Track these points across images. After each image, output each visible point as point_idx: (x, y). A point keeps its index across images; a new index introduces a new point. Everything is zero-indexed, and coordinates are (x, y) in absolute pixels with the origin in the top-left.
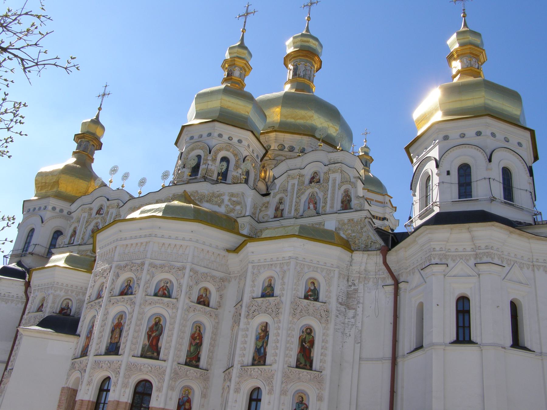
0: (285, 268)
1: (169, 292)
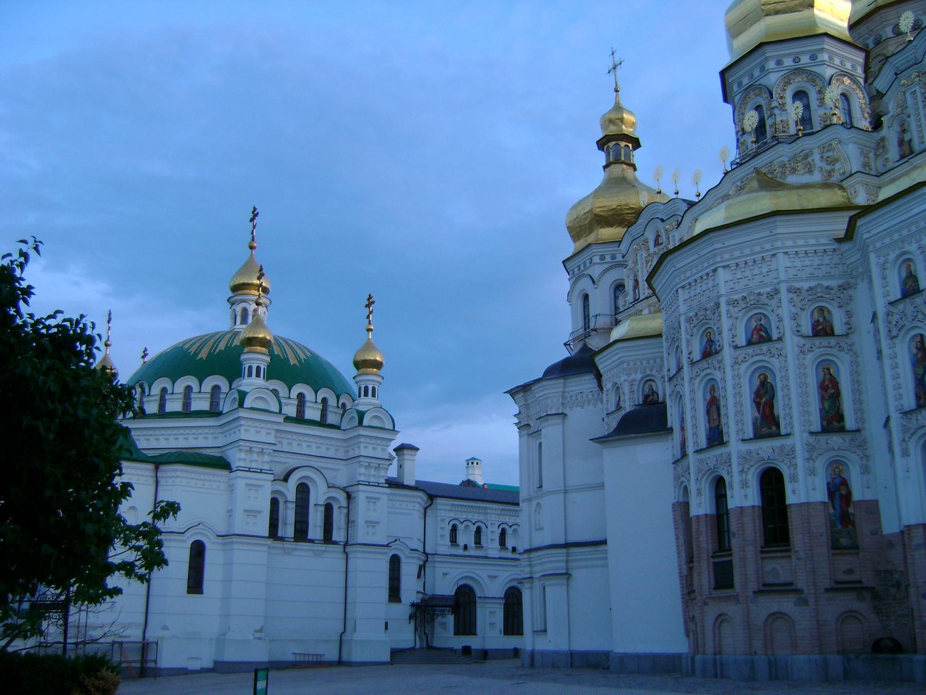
1: (766, 332)
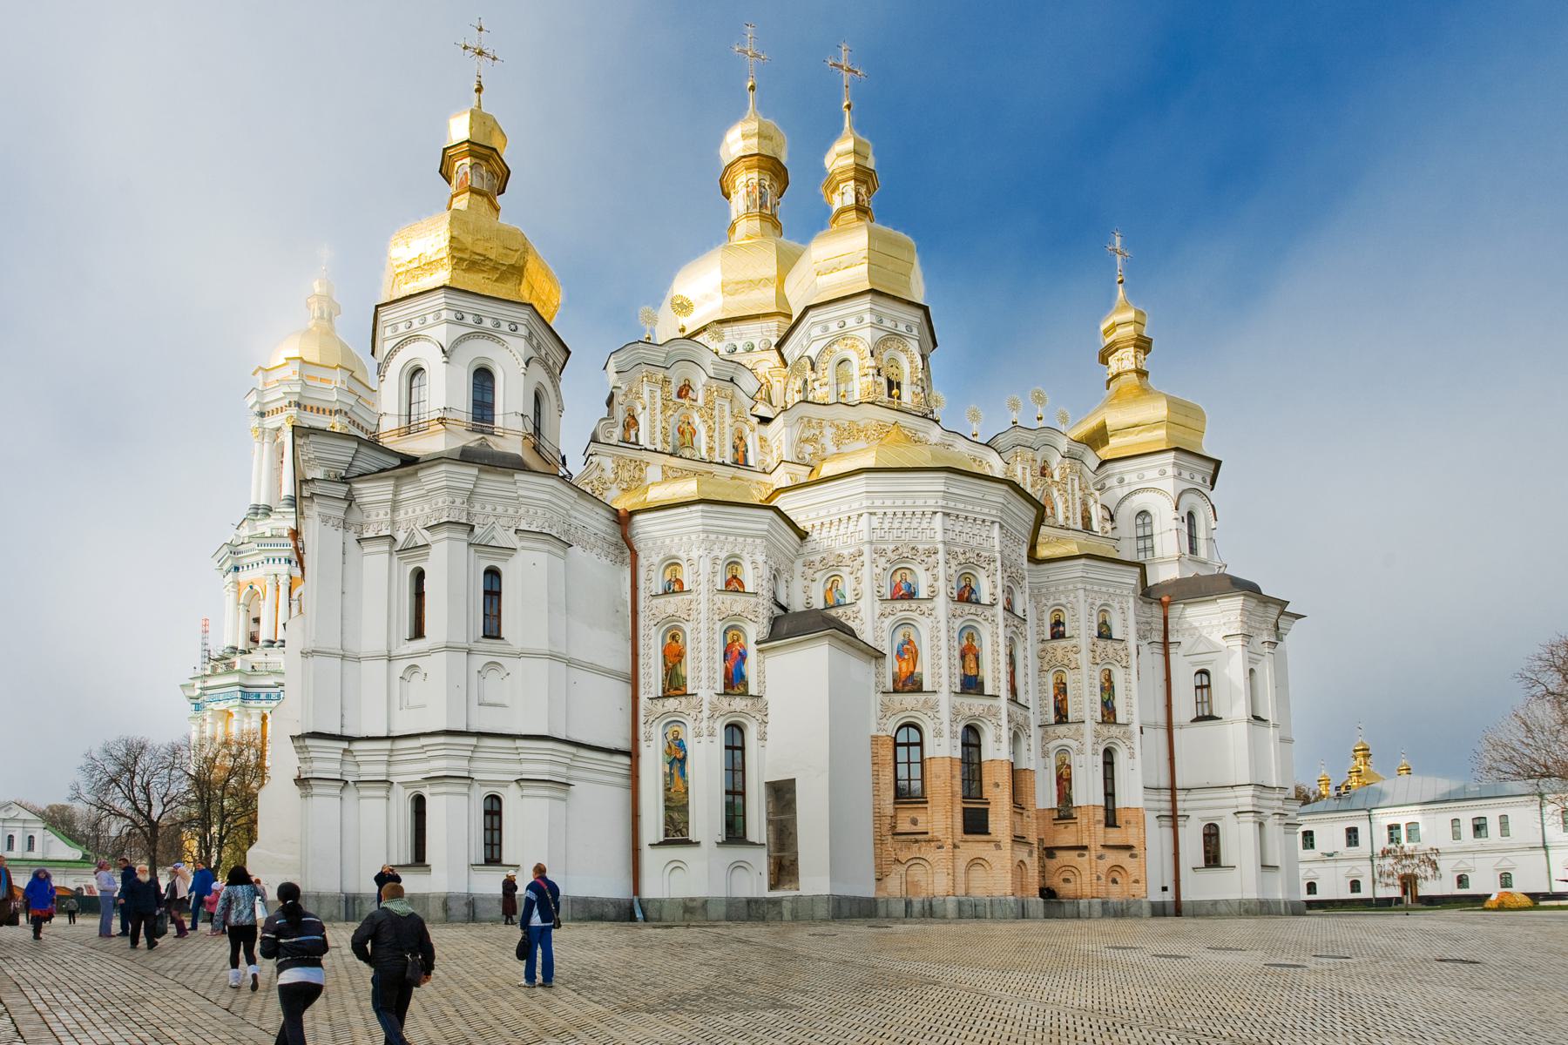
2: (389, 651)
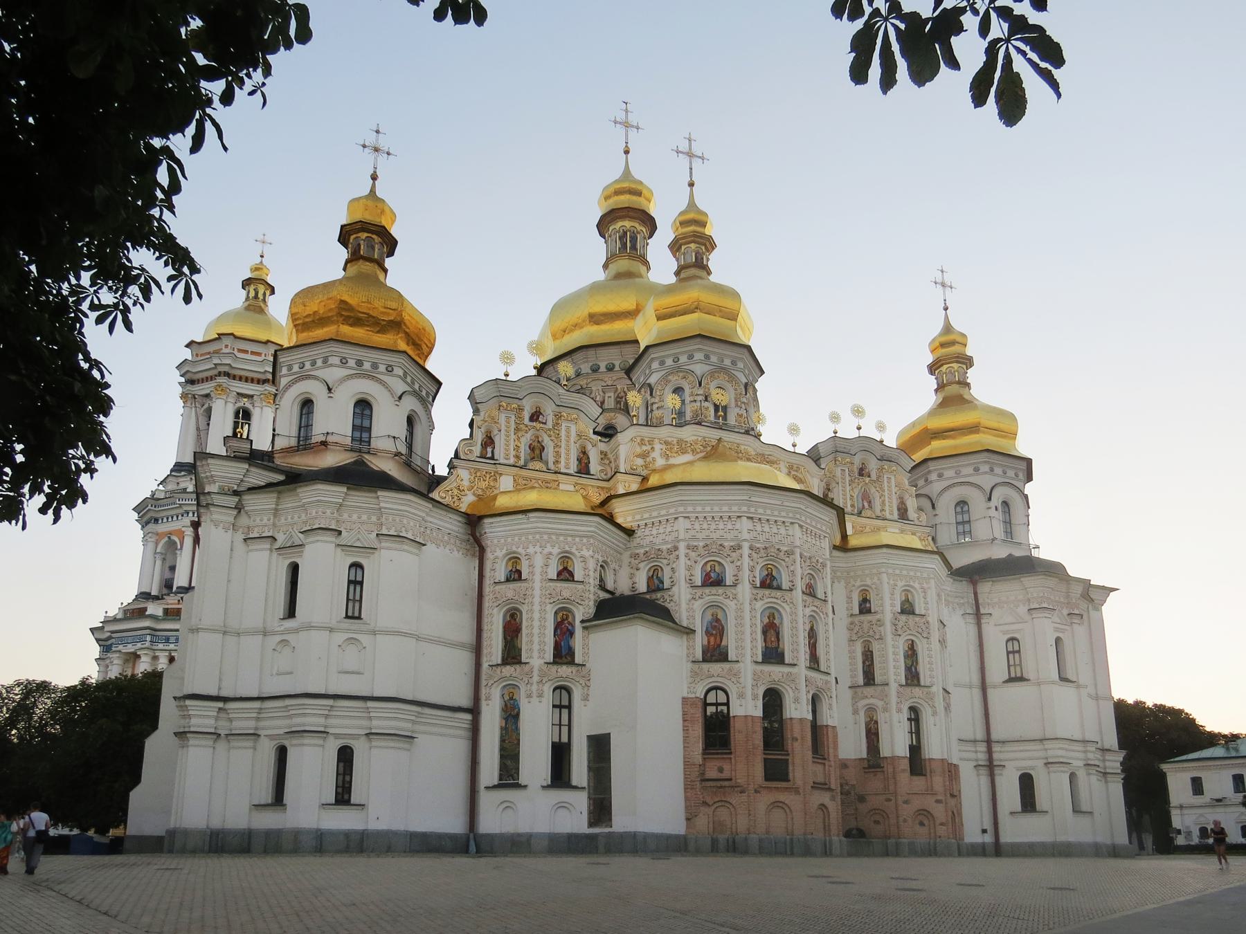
0: (925, 585)
2: (265, 628)
